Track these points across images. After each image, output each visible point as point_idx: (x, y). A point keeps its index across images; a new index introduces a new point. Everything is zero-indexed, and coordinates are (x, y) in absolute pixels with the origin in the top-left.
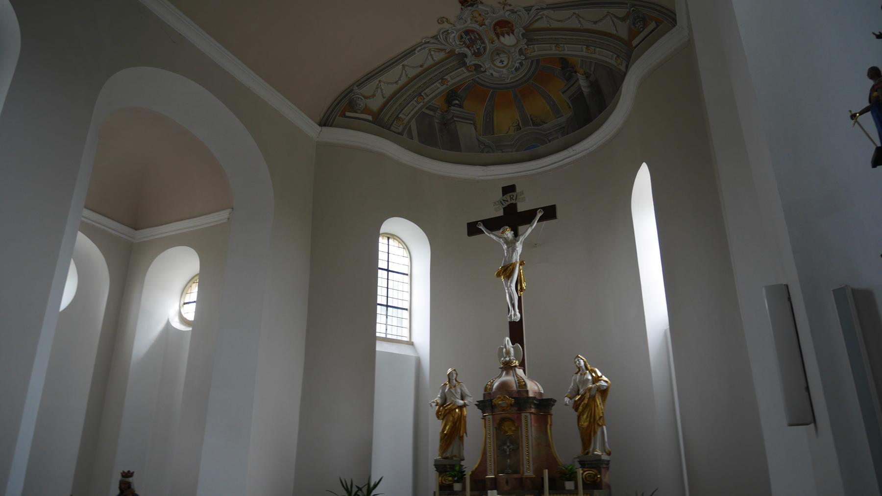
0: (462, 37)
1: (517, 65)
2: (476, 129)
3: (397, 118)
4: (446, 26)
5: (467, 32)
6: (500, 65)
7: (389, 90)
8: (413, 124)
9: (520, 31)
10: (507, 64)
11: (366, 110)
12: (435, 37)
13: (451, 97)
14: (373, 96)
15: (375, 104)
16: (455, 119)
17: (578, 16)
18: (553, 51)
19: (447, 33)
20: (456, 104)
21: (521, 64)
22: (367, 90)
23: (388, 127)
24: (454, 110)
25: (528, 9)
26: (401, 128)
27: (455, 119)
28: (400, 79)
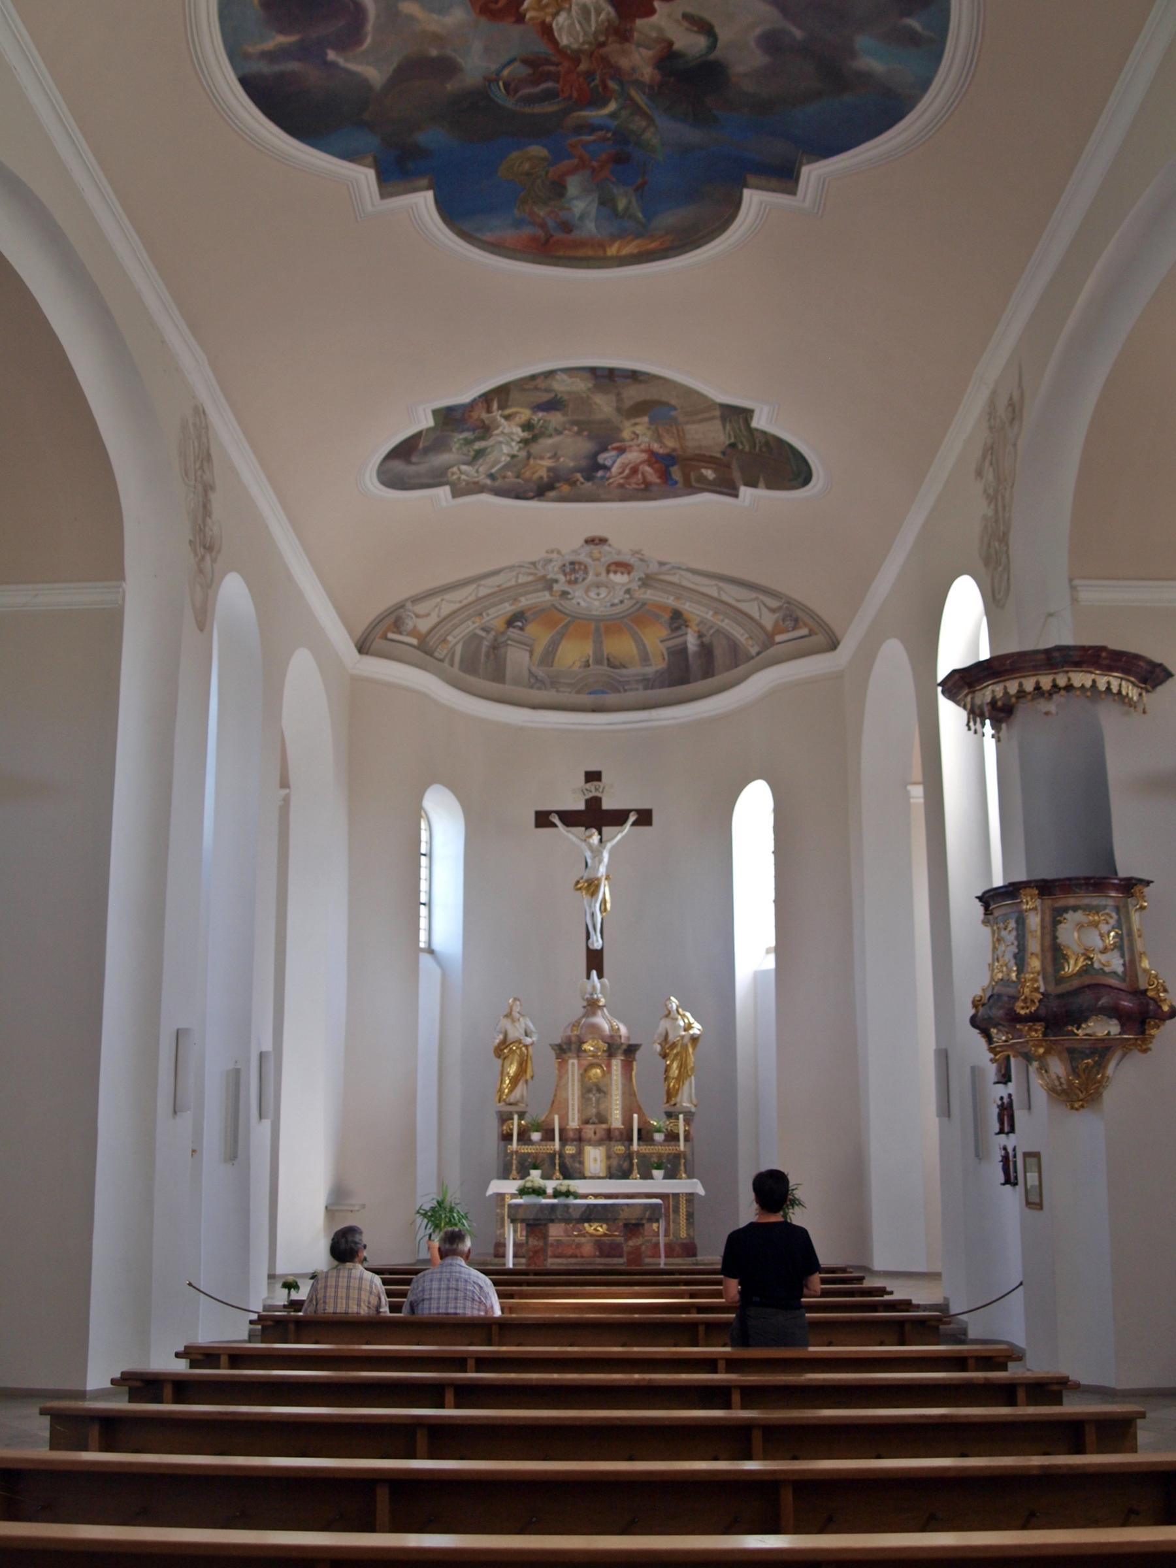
0: (564, 565)
1: (616, 601)
2: (530, 657)
3: (444, 641)
4: (554, 556)
5: (572, 563)
6: (595, 597)
7: (446, 609)
8: (459, 649)
9: (637, 574)
10: (604, 598)
11: (414, 633)
12: (534, 564)
13: (516, 620)
14: (428, 615)
15: (424, 625)
16: (509, 642)
17: (720, 589)
18: (671, 601)
19: (551, 561)
20: (518, 626)
21: (622, 602)
22: (421, 608)
23: (429, 653)
24: (513, 633)
25: (661, 564)
26: (445, 652)
27: (509, 642)
28: (466, 598)
